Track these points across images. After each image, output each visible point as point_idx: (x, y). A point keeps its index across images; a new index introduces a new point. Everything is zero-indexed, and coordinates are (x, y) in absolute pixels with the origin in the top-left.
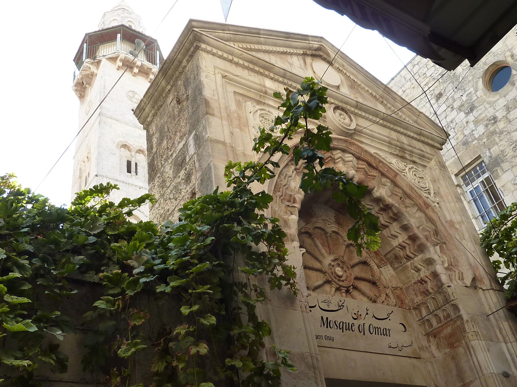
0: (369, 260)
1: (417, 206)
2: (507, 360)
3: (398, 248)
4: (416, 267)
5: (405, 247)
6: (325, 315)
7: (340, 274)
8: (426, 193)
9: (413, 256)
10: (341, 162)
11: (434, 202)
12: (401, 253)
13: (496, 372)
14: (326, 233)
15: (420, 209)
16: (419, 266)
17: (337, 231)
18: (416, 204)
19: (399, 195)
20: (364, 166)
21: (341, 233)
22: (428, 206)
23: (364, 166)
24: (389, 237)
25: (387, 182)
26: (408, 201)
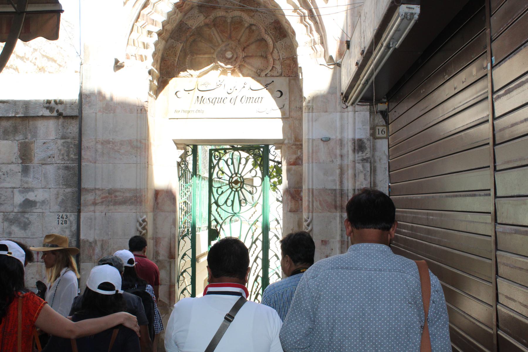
6: (200, 94)
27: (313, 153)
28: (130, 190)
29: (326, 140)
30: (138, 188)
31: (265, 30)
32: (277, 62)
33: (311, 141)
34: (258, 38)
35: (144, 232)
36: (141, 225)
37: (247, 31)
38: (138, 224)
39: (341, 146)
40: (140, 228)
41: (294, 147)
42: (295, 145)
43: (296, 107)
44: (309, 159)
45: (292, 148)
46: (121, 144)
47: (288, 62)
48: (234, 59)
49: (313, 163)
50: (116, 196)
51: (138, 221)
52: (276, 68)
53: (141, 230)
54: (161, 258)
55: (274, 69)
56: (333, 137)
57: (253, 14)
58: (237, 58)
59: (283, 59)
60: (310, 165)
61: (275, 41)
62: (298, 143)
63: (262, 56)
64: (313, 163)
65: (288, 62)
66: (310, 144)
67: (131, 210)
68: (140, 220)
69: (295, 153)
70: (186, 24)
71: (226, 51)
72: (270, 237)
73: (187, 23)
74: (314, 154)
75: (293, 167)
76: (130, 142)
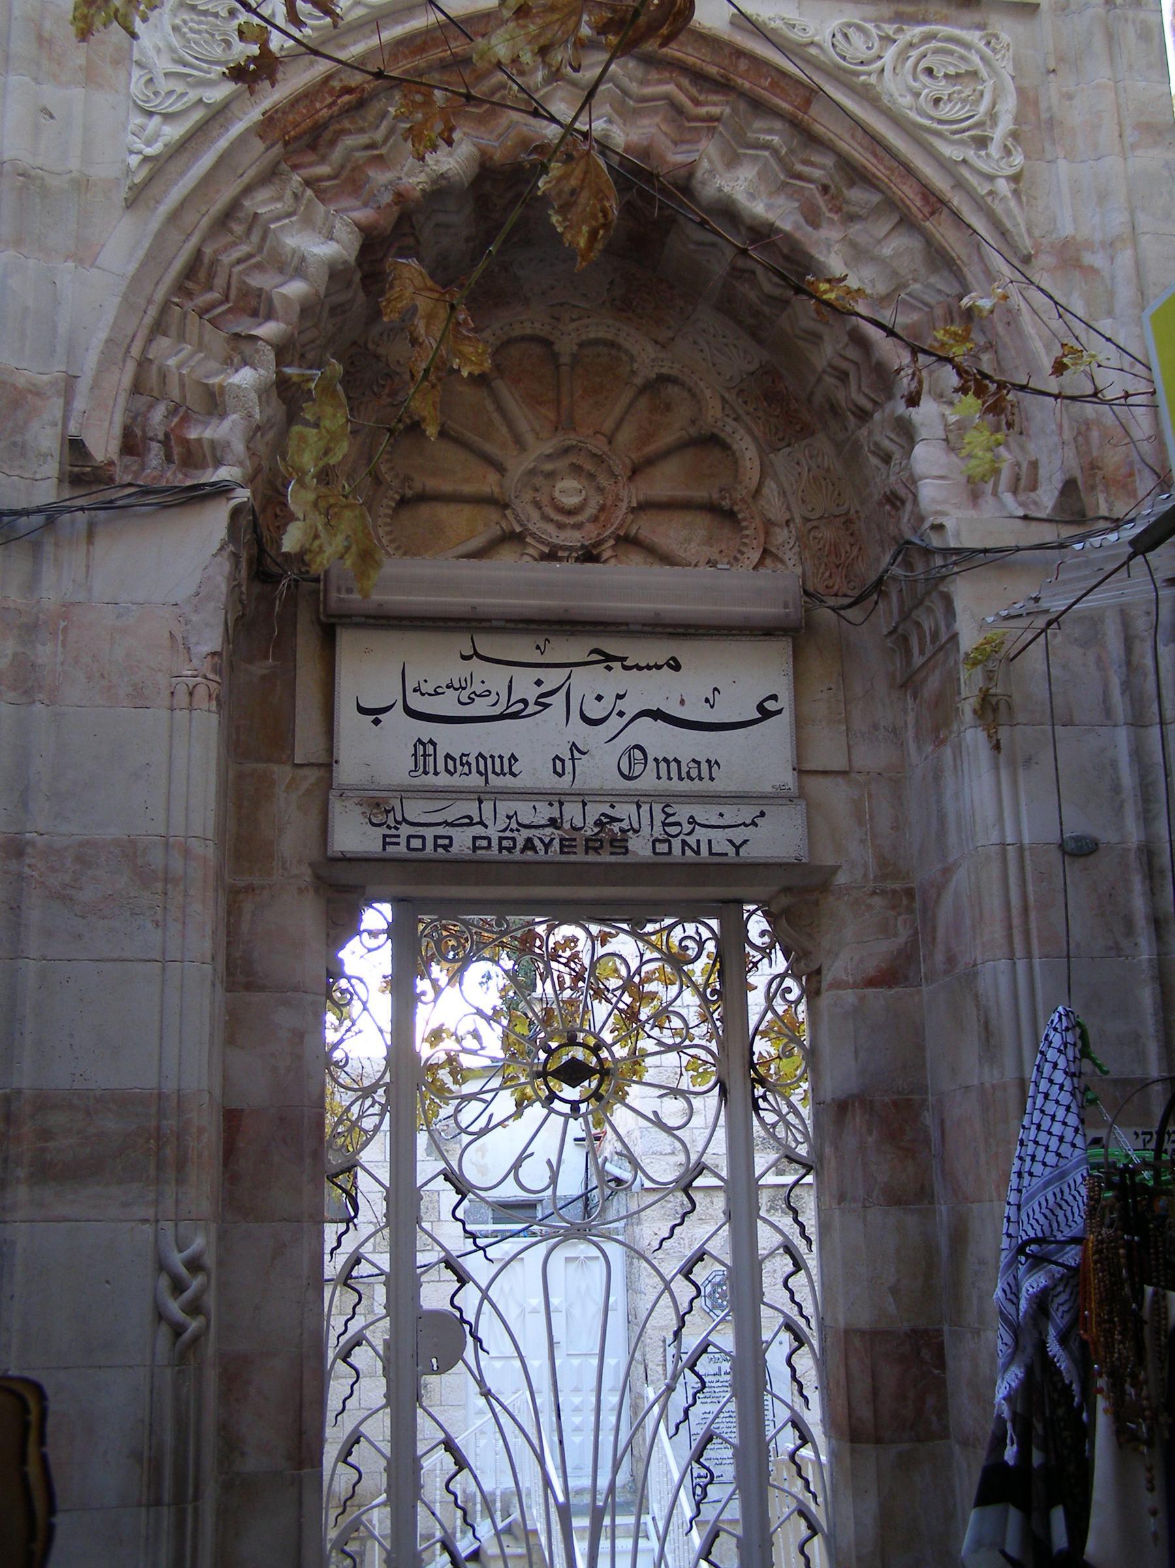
0: (728, 429)
1: (897, 207)
2: (1116, 789)
3: (830, 375)
4: (876, 444)
5: (847, 375)
7: (571, 501)
8: (962, 142)
9: (869, 406)
10: (560, 94)
11: (991, 178)
12: (841, 395)
13: (1026, 840)
14: (555, 356)
15: (906, 222)
16: (886, 444)
17: (609, 337)
18: (891, 204)
19: (817, 173)
20: (670, 88)
21: (627, 345)
22: (935, 201)
23: (670, 88)
24: (797, 337)
25: (770, 131)
26: (857, 195)
27: (1025, 909)
28: (121, 1101)
29: (1079, 850)
30: (170, 1086)
31: (724, 400)
32: (781, 535)
33: (1011, 852)
34: (693, 431)
35: (194, 1325)
36: (178, 1287)
37: (643, 402)
38: (164, 1282)
39: (1151, 878)
40: (174, 1308)
41: (877, 901)
42: (883, 892)
43: (875, 727)
44: (1010, 938)
45: (870, 907)
46: (80, 859)
47: (827, 533)
48: (591, 510)
49: (1029, 956)
50: (45, 1134)
51: (162, 1266)
52: (777, 558)
53: (180, 1316)
54: (252, 1463)
55: (768, 561)
56: (1107, 836)
57: (670, 334)
58: (602, 508)
59: (806, 520)
60: (1021, 965)
61: (767, 449)
62: (897, 886)
63: (711, 508)
64: (1029, 956)
65: (827, 533)
66: (1013, 870)
67: (126, 1205)
68: (177, 1259)
69: (885, 929)
70: (377, 357)
71: (551, 475)
72: (766, 1336)
73: (382, 351)
74: (1033, 915)
75: (878, 997)
76: (130, 852)
